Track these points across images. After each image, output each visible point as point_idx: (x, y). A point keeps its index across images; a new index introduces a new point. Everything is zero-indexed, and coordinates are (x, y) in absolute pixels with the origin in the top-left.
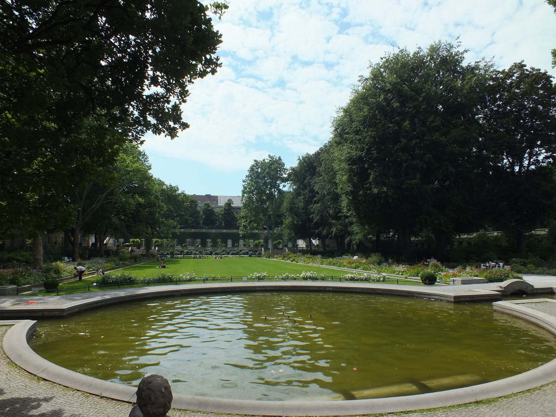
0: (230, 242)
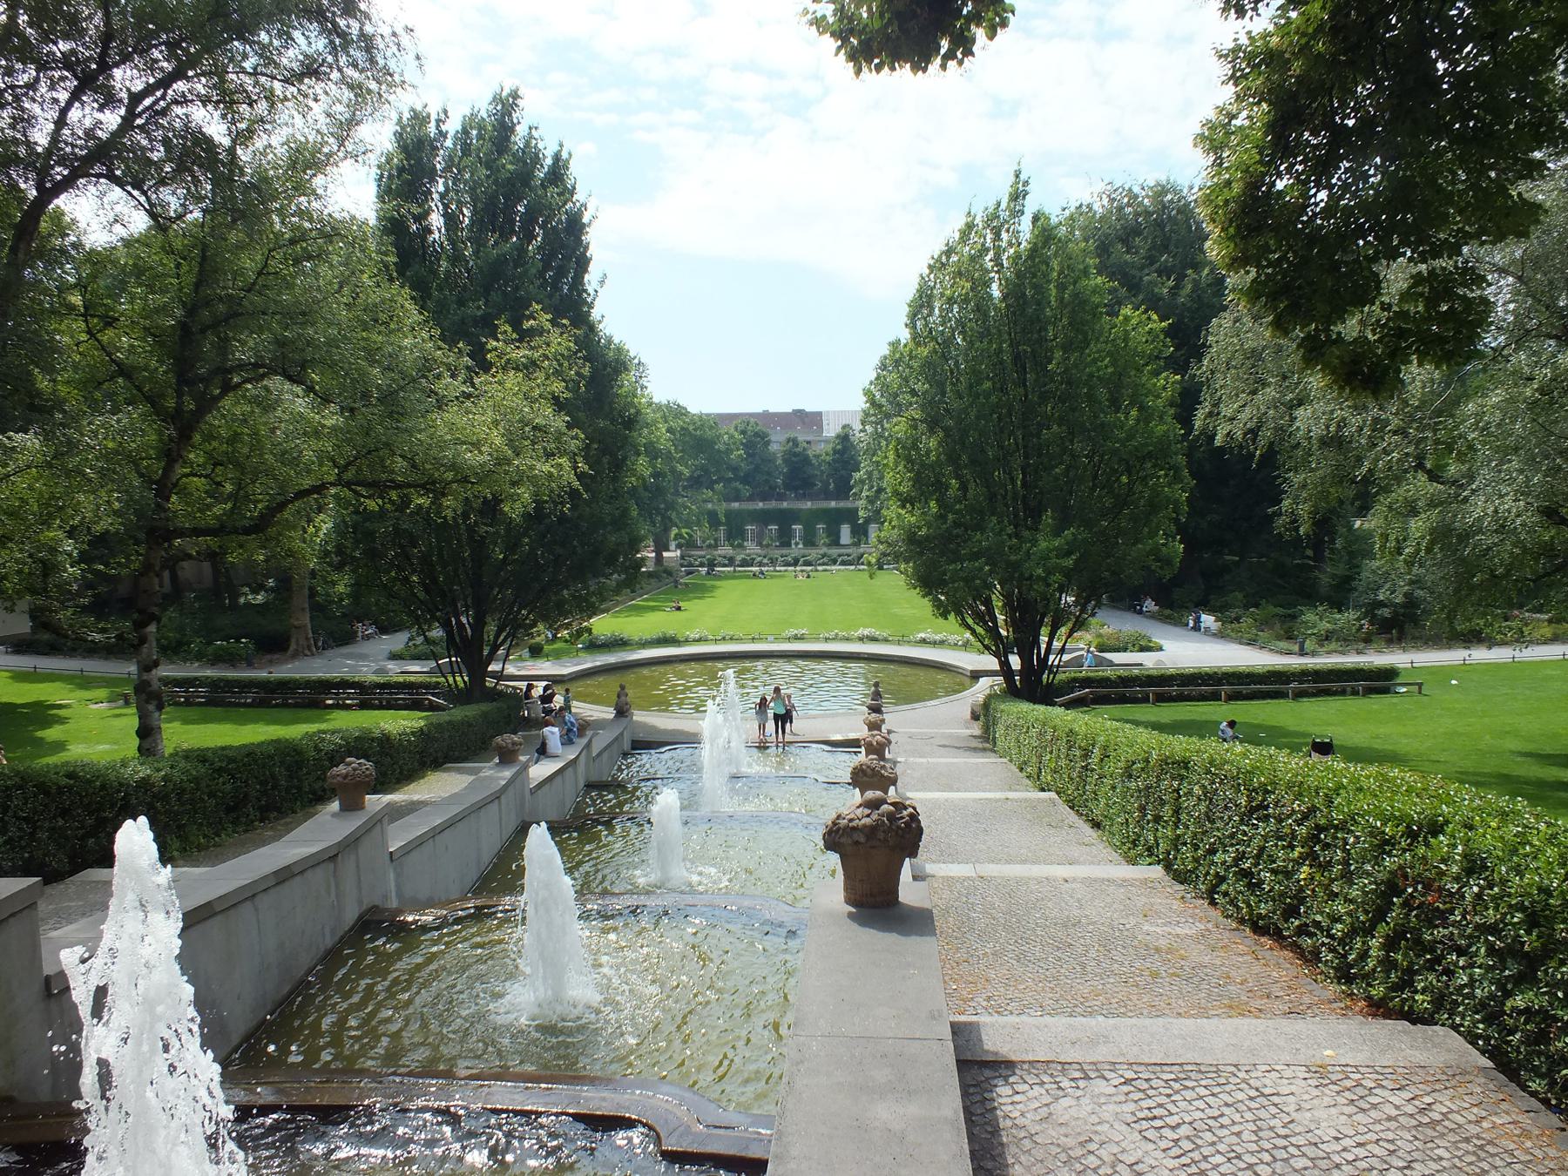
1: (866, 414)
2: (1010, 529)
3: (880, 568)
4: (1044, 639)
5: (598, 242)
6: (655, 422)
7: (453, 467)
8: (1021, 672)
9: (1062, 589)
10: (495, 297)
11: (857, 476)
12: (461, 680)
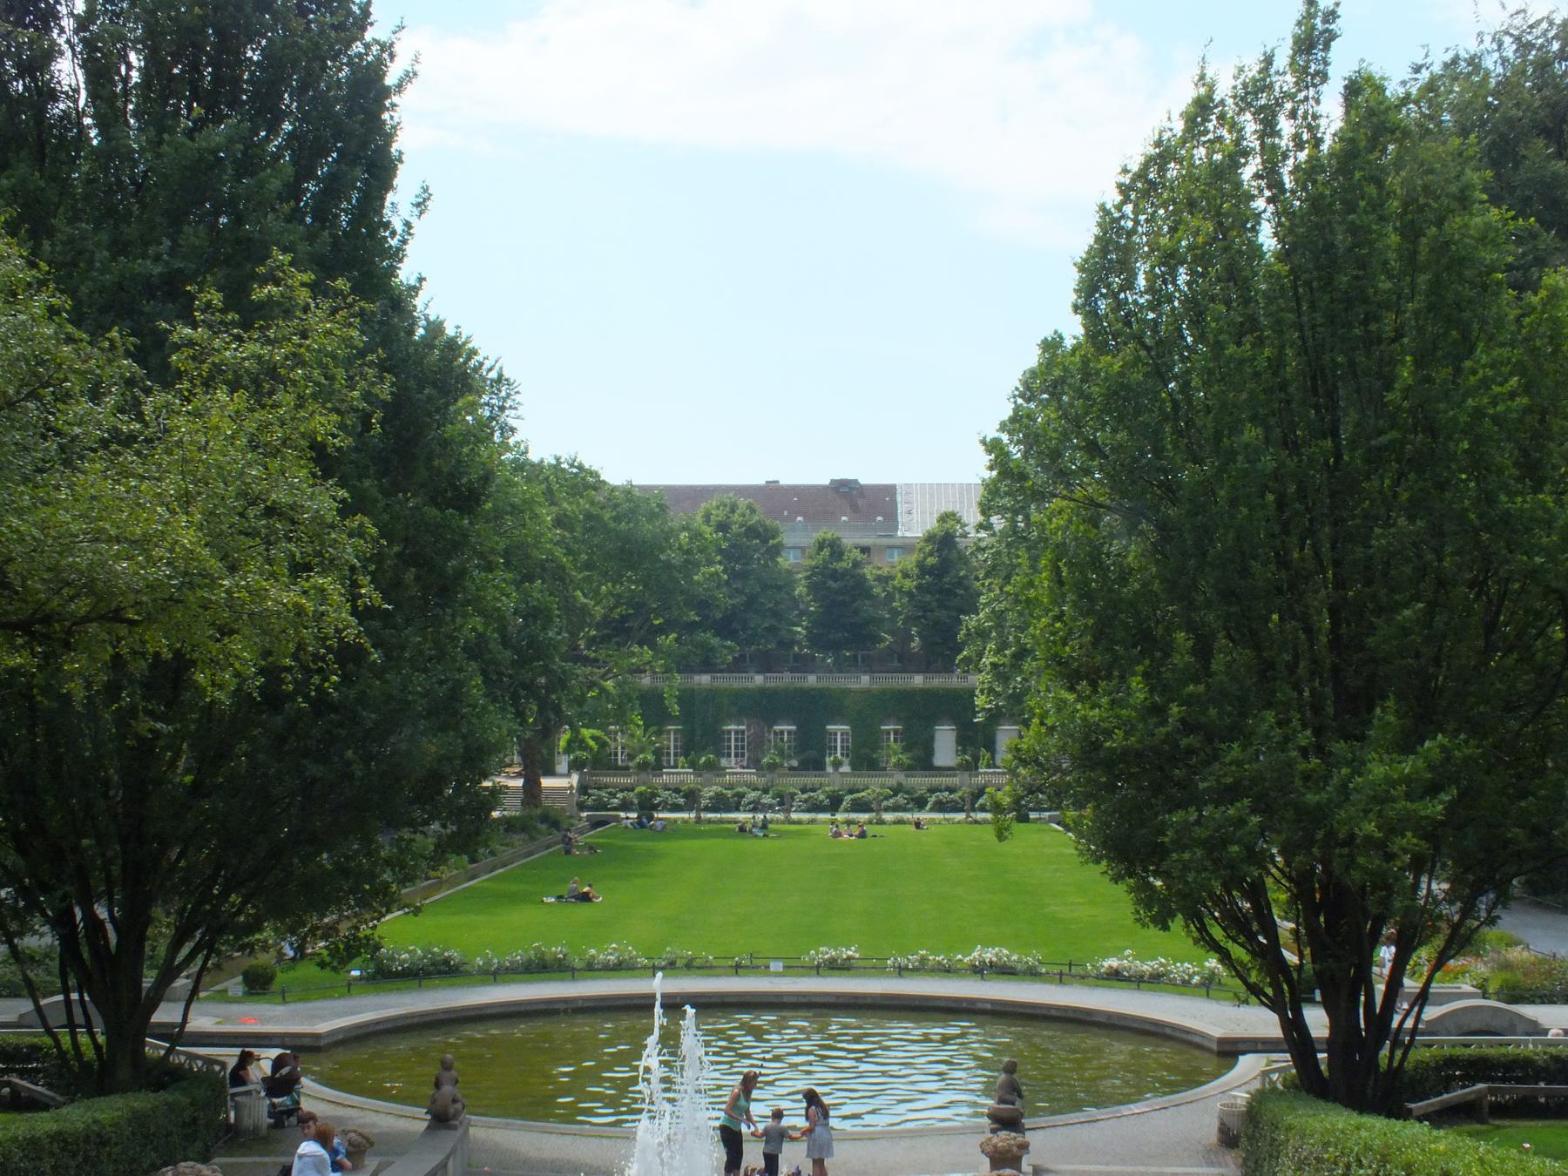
1: (992, 489)
2: (1305, 738)
3: (1023, 819)
5: (417, 129)
6: (528, 503)
7: (90, 587)
8: (1330, 1044)
9: (1420, 865)
10: (194, 235)
11: (971, 621)
12: (90, 1041)
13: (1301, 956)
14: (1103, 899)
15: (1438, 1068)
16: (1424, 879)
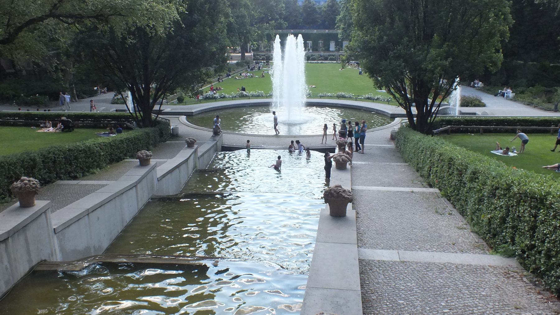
0: (332, 46)
4: (430, 101)
8: (417, 116)
11: (338, 18)
13: (411, 96)
14: (367, 81)
15: (440, 122)
16: (441, 80)
